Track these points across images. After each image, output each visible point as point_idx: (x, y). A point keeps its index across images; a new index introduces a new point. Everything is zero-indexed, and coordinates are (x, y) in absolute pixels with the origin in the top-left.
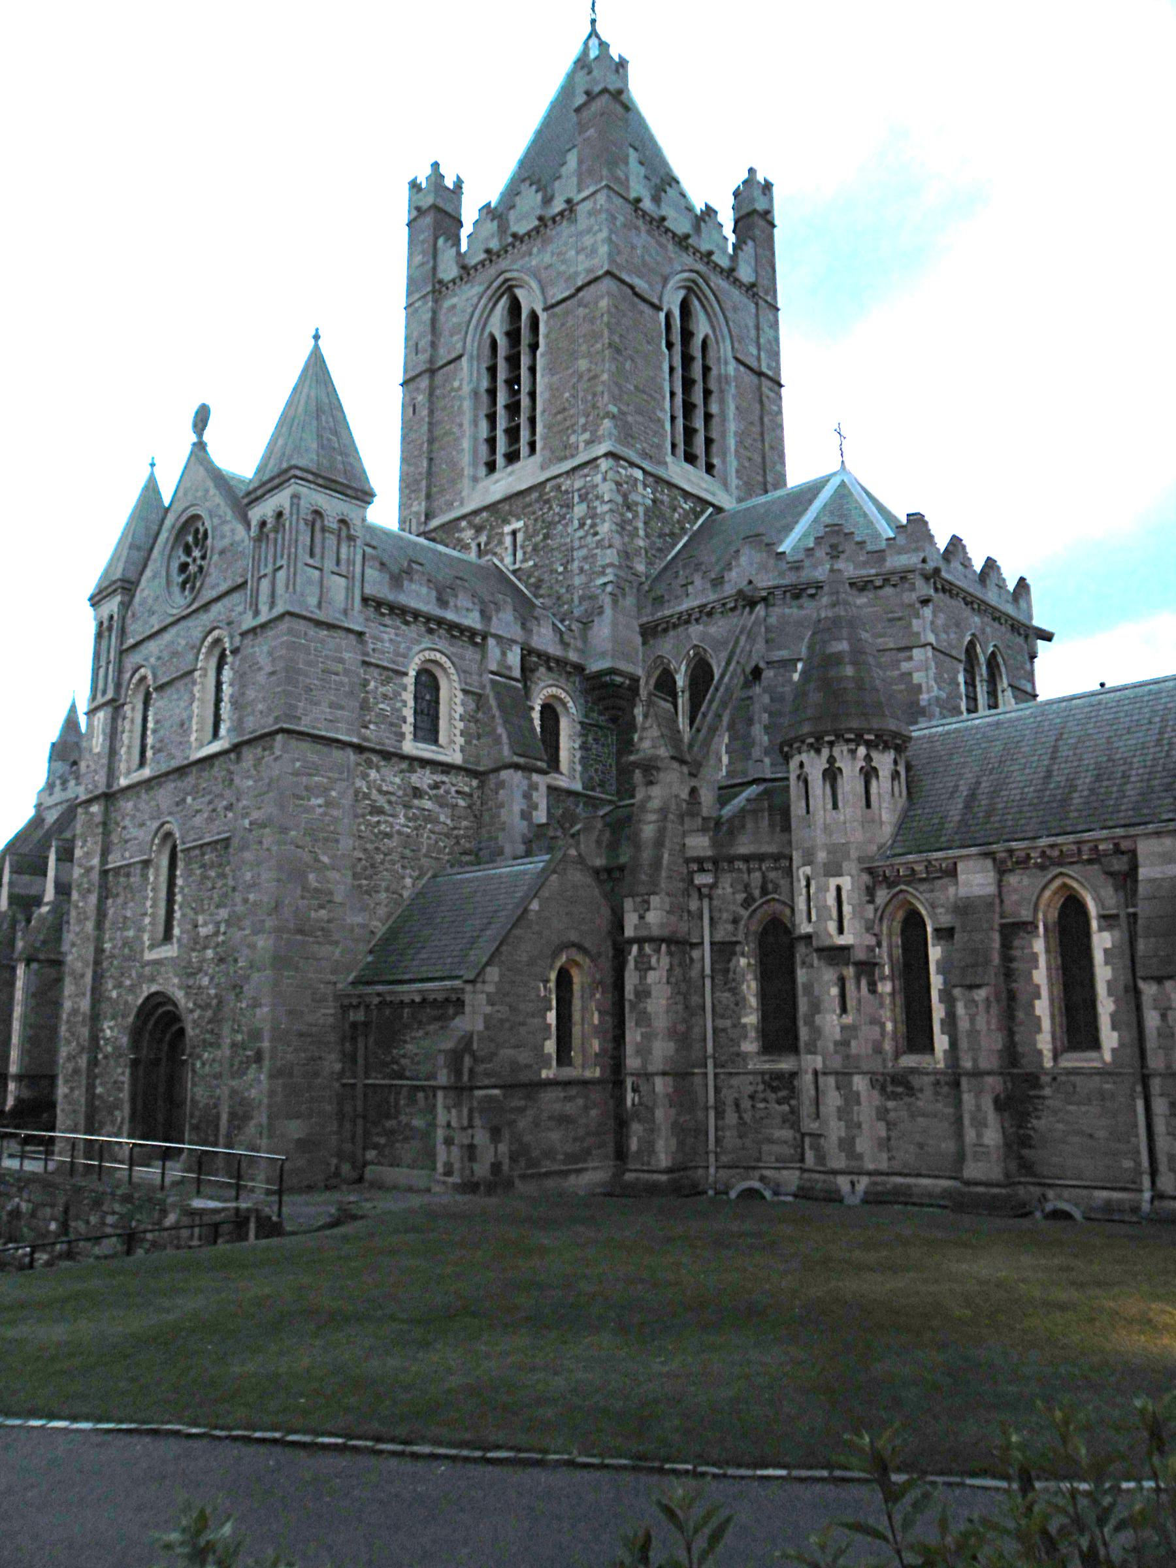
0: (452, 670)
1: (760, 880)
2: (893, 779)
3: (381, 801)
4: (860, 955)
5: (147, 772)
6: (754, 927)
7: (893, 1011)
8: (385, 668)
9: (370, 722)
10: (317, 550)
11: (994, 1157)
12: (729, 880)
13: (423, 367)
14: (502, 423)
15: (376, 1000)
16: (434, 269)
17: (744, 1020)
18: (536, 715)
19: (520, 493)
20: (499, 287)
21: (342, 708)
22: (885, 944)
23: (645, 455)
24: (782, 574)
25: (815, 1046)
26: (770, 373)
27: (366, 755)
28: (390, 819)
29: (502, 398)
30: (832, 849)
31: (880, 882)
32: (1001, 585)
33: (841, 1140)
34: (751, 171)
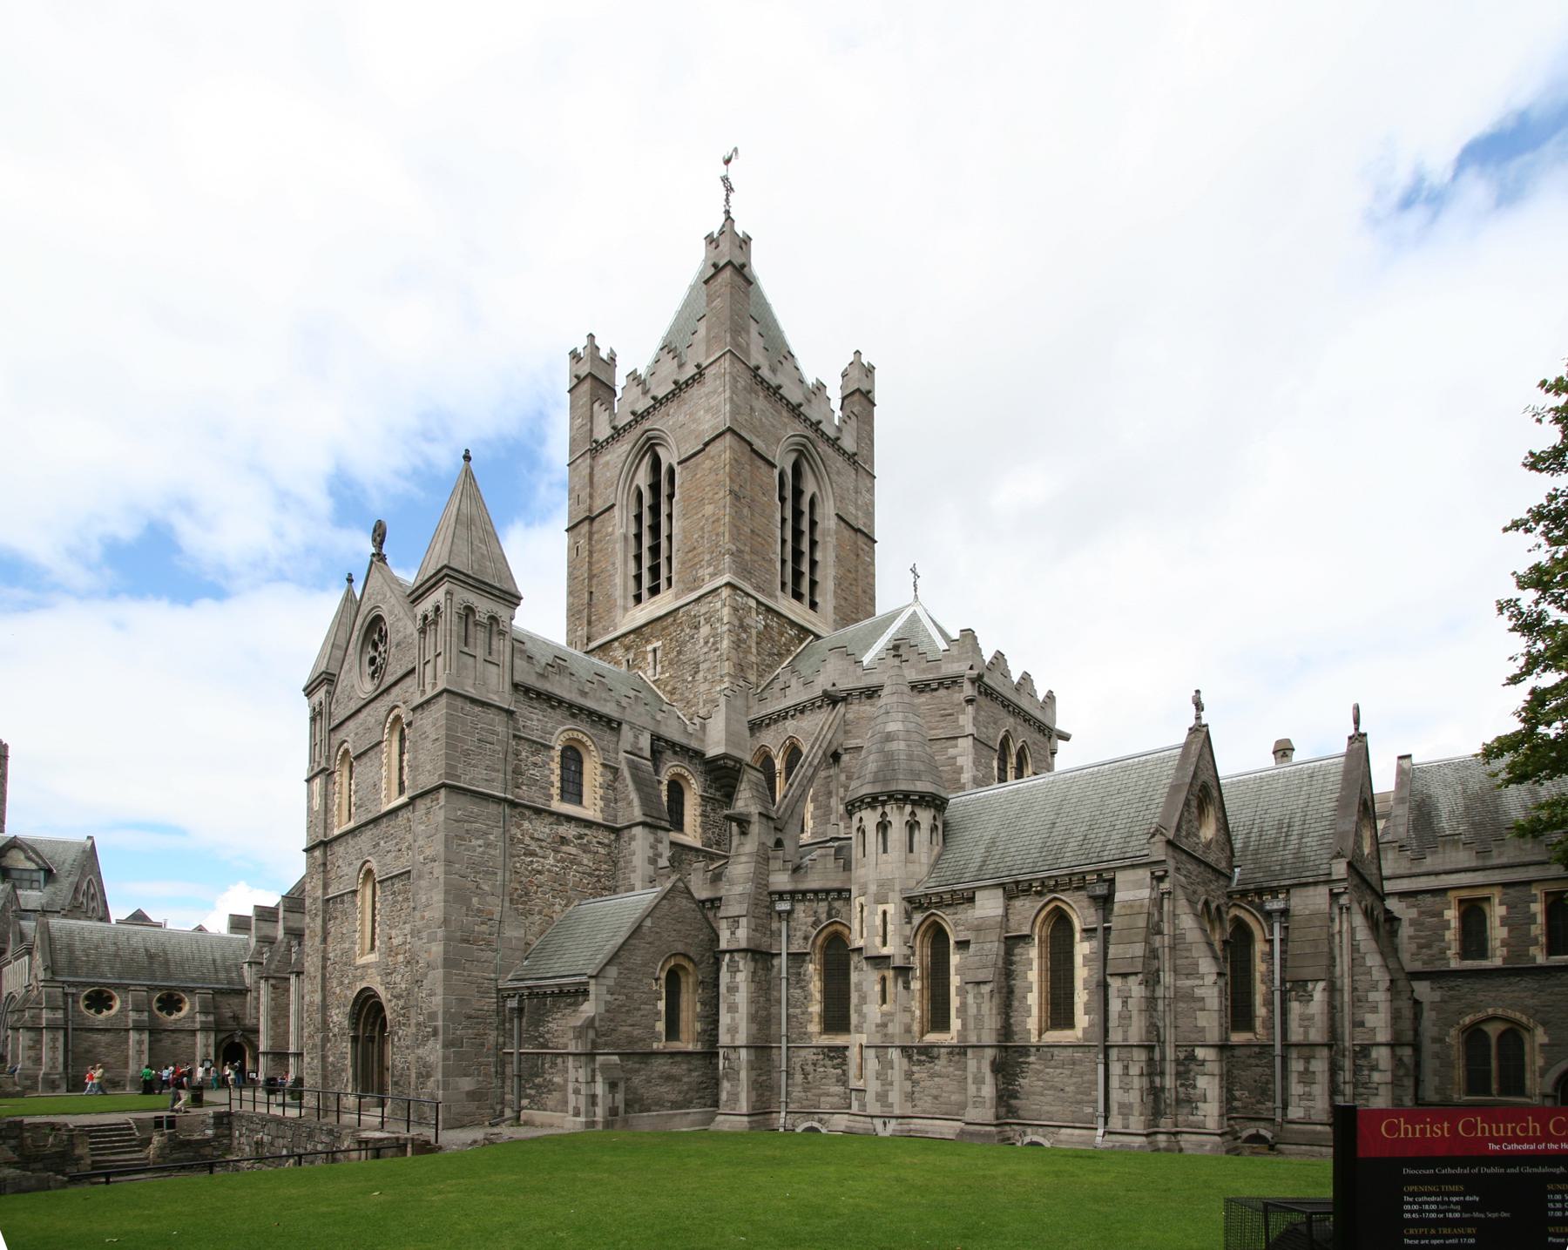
1: (826, 909)
3: (534, 846)
4: (898, 962)
5: (352, 825)
7: (921, 1002)
14: (646, 563)
15: (526, 992)
18: (664, 788)
19: (660, 618)
22: (917, 953)
23: (758, 588)
25: (862, 1027)
26: (866, 531)
28: (542, 860)
29: (647, 541)
30: (882, 884)
31: (916, 908)
32: (1033, 695)
33: (878, 1094)
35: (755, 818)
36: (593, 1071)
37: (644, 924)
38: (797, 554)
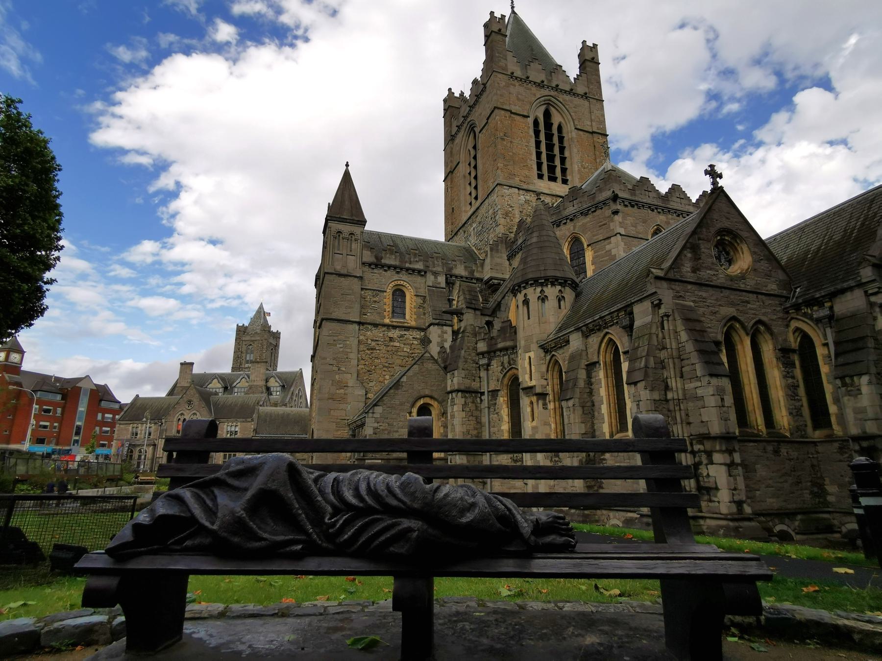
0: (410, 288)
2: (559, 301)
4: (538, 390)
6: (506, 381)
8: (374, 290)
16: (451, 131)
17: (502, 428)
27: (365, 326)
28: (378, 351)
34: (584, 42)
37: (402, 380)
38: (550, 158)
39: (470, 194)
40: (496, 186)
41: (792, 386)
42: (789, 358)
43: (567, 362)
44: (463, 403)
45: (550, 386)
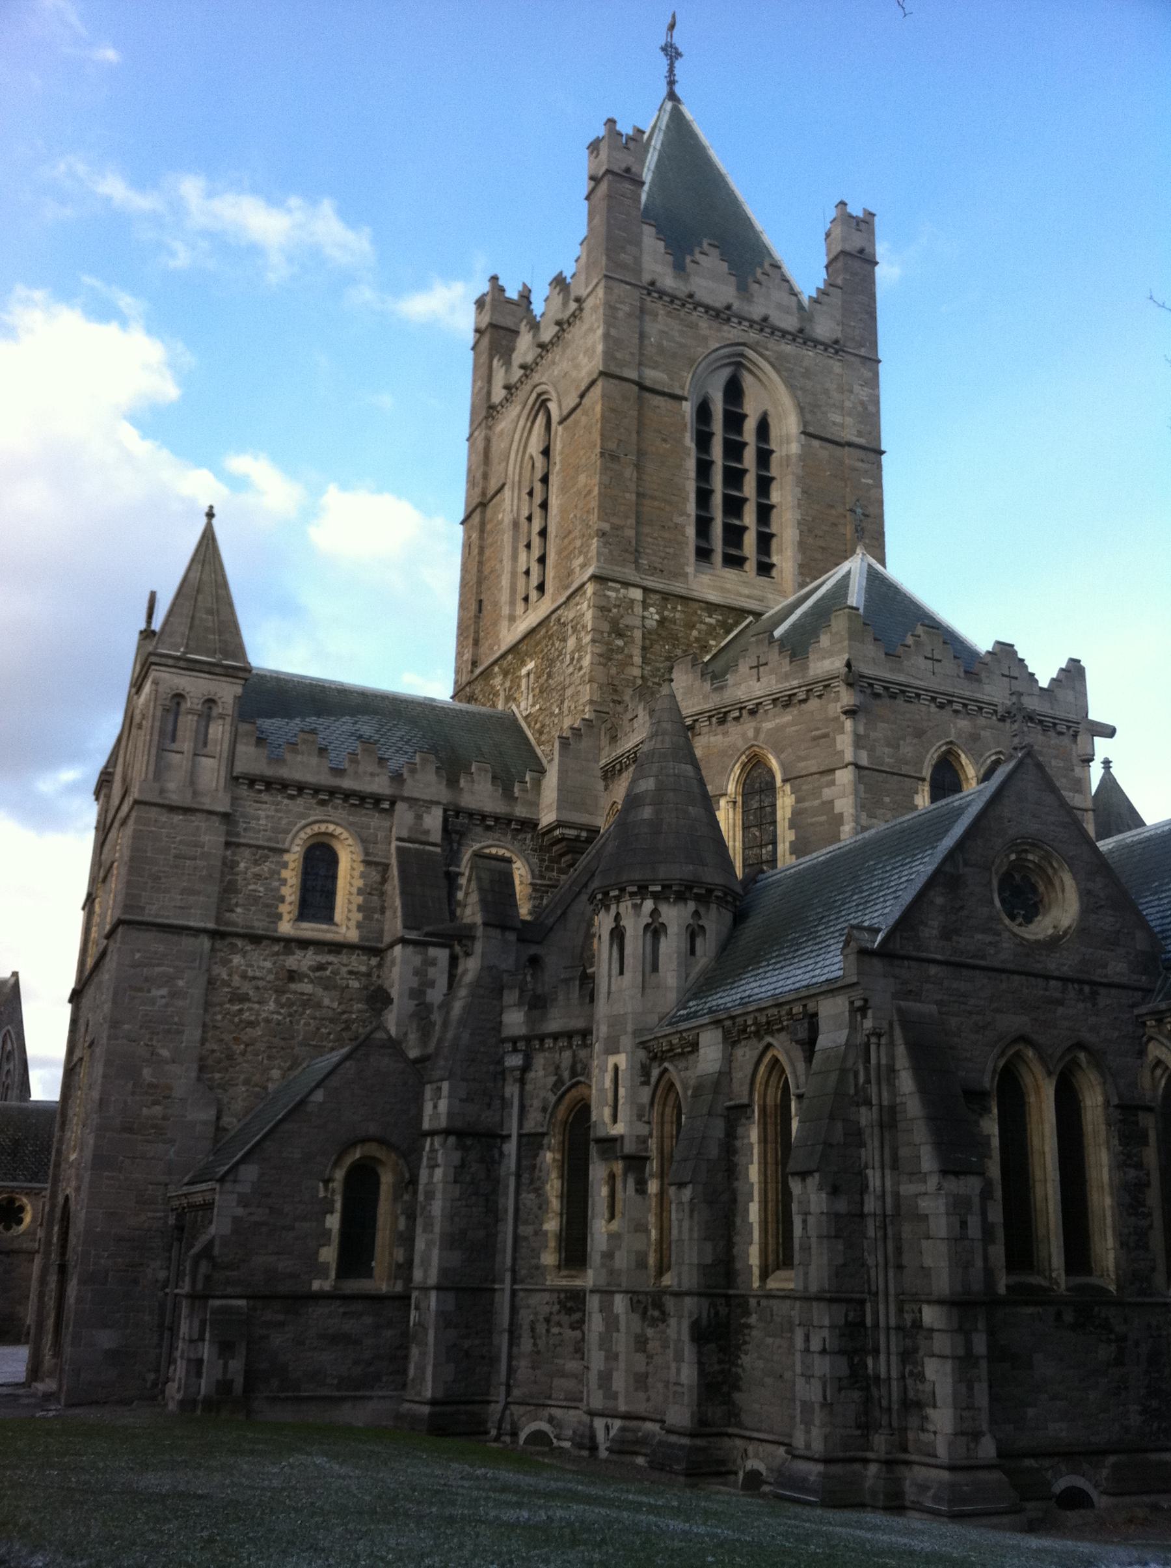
3: (247, 988)
4: (629, 1148)
8: (259, 847)
9: (237, 905)
10: (179, 733)
11: (686, 1399)
12: (542, 1061)
13: (476, 501)
16: (489, 393)
20: (534, 404)
21: (199, 893)
23: (654, 570)
24: (706, 697)
27: (229, 940)
28: (256, 1006)
35: (479, 932)
36: (203, 1323)
38: (734, 506)
39: (527, 573)
40: (590, 579)
41: (1136, 1184)
42: (1137, 1123)
43: (690, 1093)
44: (457, 1162)
45: (654, 1140)
